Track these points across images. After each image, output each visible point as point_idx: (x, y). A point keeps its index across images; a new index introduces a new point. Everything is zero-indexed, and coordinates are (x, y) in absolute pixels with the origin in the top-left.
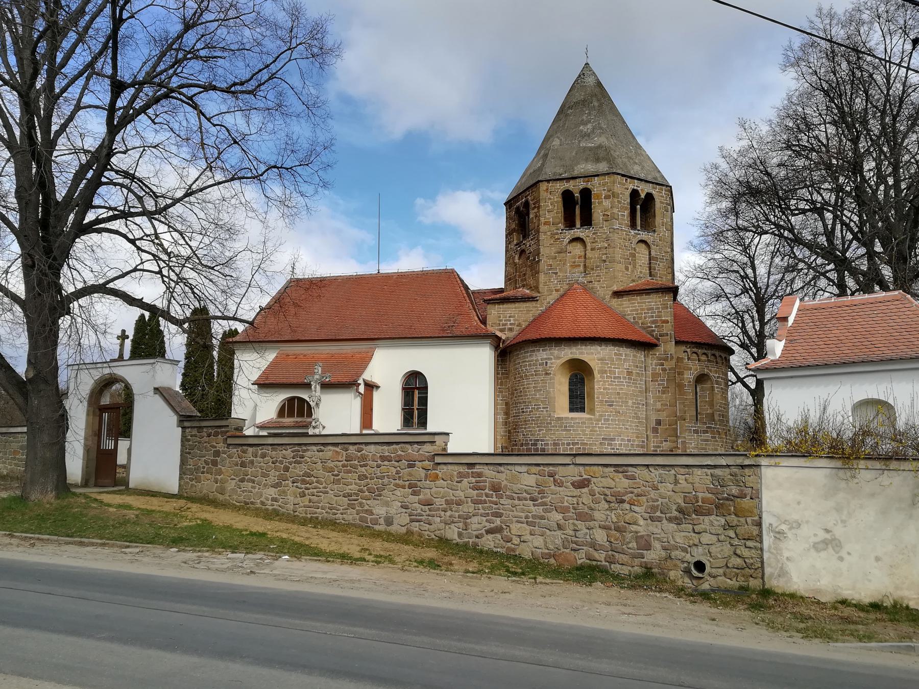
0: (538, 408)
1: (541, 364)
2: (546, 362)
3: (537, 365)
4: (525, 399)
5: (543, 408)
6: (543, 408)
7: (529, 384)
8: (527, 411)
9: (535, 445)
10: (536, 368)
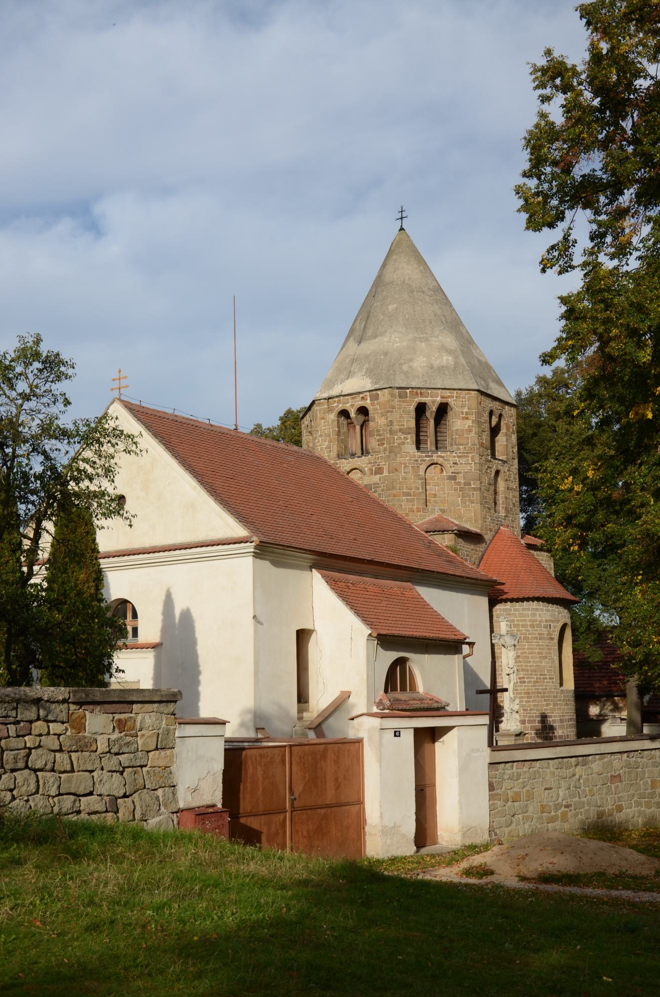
0: (544, 678)
2: (550, 625)
3: (541, 627)
5: (550, 678)
6: (550, 678)
7: (532, 649)
10: (540, 630)
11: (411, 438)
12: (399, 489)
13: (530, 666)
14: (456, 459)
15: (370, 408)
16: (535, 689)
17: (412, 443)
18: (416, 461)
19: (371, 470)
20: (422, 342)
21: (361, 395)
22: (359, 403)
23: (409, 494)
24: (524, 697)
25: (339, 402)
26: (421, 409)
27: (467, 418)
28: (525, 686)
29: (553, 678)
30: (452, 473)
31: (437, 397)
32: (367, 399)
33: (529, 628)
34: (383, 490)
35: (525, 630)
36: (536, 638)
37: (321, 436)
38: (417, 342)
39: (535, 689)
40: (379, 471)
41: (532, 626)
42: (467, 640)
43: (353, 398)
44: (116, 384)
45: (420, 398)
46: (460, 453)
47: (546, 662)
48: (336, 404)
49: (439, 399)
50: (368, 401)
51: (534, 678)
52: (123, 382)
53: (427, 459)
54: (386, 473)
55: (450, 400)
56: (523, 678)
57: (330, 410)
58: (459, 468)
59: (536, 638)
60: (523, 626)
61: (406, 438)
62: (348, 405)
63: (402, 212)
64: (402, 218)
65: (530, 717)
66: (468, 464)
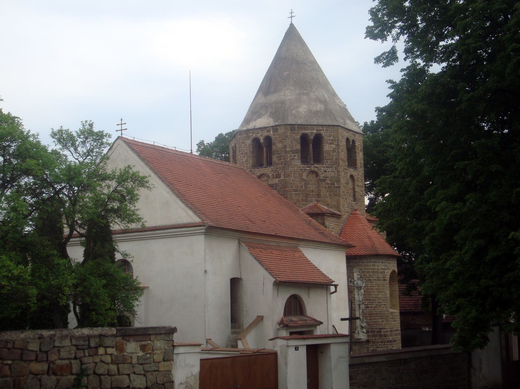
1: (381, 273)
2: (384, 271)
4: (369, 297)
5: (384, 305)
6: (384, 305)
7: (373, 286)
8: (371, 307)
9: (380, 332)
10: (378, 275)
11: (298, 156)
12: (291, 187)
13: (372, 297)
14: (326, 168)
15: (273, 137)
16: (375, 312)
17: (298, 159)
18: (301, 170)
19: (273, 175)
20: (304, 96)
21: (267, 129)
22: (266, 134)
23: (296, 191)
24: (368, 317)
25: (253, 133)
26: (304, 139)
27: (332, 143)
28: (369, 310)
29: (386, 305)
30: (323, 177)
31: (314, 130)
32: (270, 132)
33: (371, 274)
34: (280, 188)
35: (369, 275)
36: (375, 280)
37: (242, 154)
38: (302, 96)
39: (375, 312)
40: (278, 176)
41: (373, 272)
42: (333, 283)
43: (262, 131)
44: (119, 128)
45: (303, 131)
46: (328, 165)
47: (381, 295)
48: (251, 134)
49: (315, 131)
50: (271, 133)
51: (374, 305)
52: (124, 127)
53: (308, 169)
54: (282, 178)
55: (322, 132)
56: (368, 304)
57: (248, 138)
58: (327, 174)
59: (375, 280)
60: (367, 272)
61: (295, 156)
62: (259, 135)
63: (292, 13)
64: (292, 17)
65: (372, 329)
66: (333, 172)
